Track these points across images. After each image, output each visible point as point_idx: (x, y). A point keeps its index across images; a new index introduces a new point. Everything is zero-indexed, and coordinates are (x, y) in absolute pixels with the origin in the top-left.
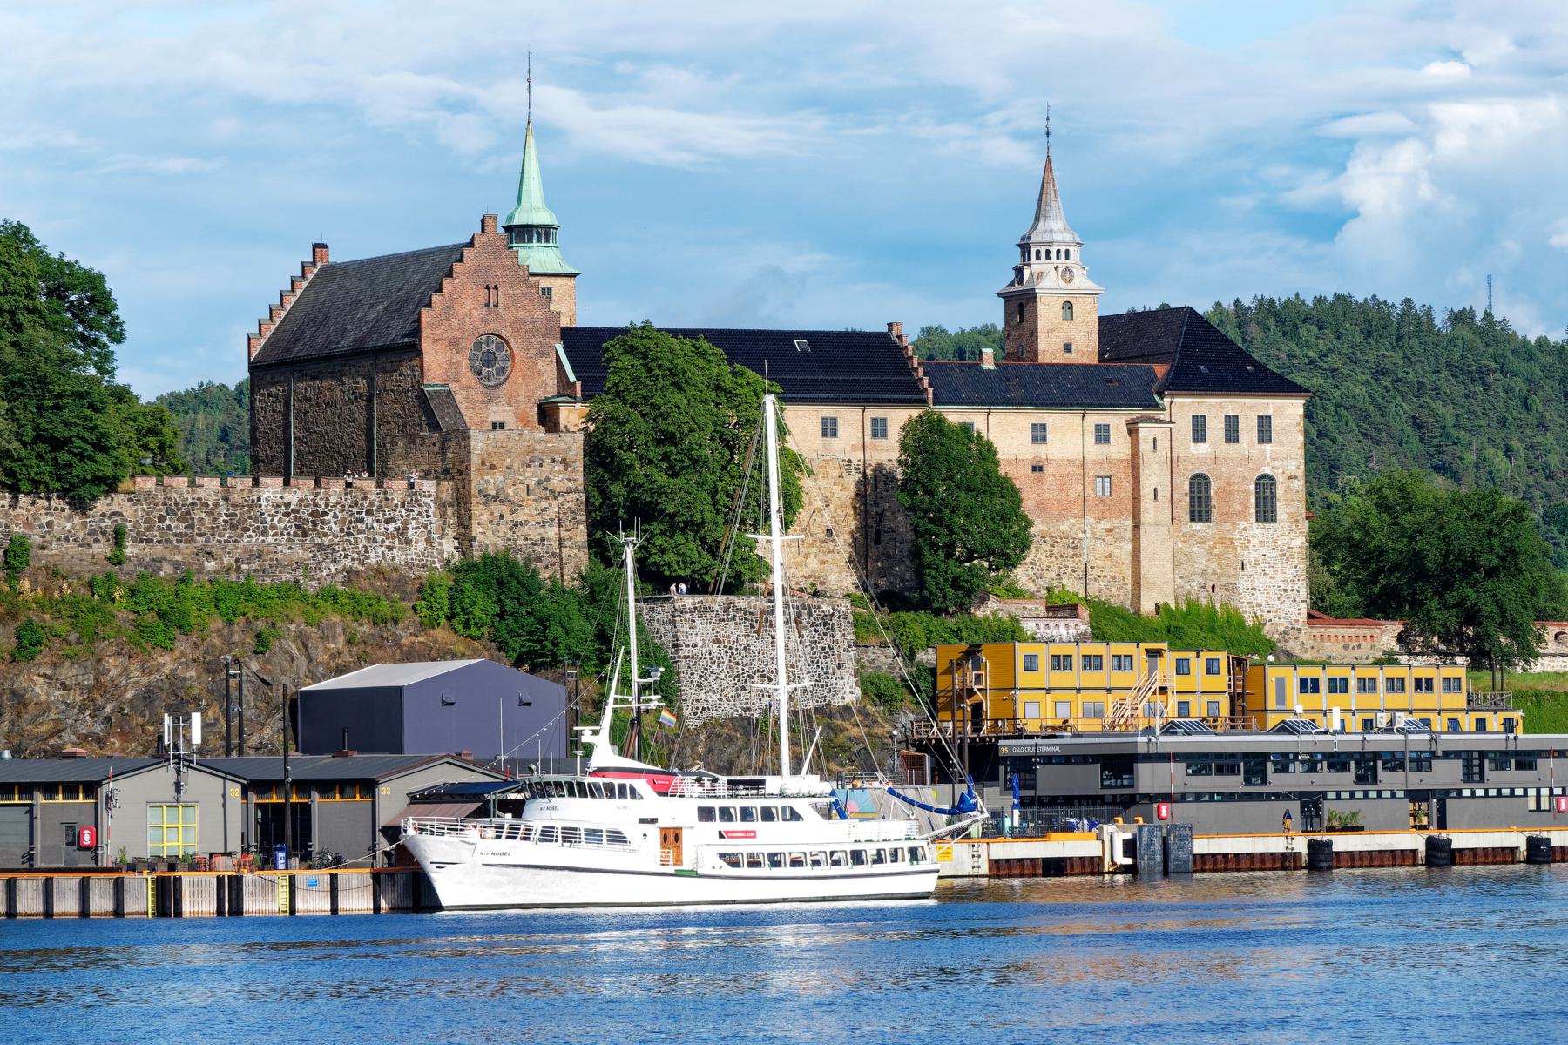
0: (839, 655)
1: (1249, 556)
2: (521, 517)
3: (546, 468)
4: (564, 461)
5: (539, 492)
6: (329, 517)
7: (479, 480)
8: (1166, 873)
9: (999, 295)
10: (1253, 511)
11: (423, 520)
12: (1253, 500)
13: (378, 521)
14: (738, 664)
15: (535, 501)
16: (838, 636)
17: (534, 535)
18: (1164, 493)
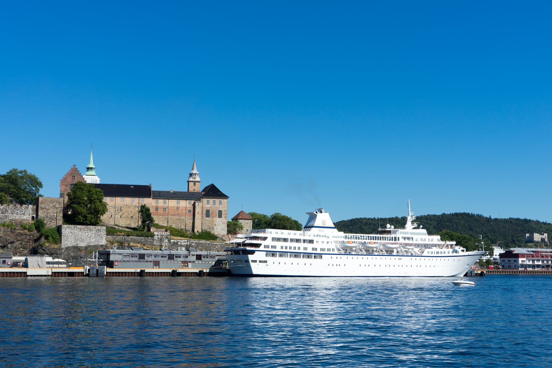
0: (102, 236)
1: (216, 223)
2: (49, 211)
3: (55, 203)
4: (59, 203)
5: (53, 208)
6: (9, 211)
7: (40, 205)
8: (97, 276)
10: (218, 216)
11: (29, 212)
12: (218, 214)
14: (76, 237)
16: (102, 233)
17: (52, 215)
18: (200, 213)
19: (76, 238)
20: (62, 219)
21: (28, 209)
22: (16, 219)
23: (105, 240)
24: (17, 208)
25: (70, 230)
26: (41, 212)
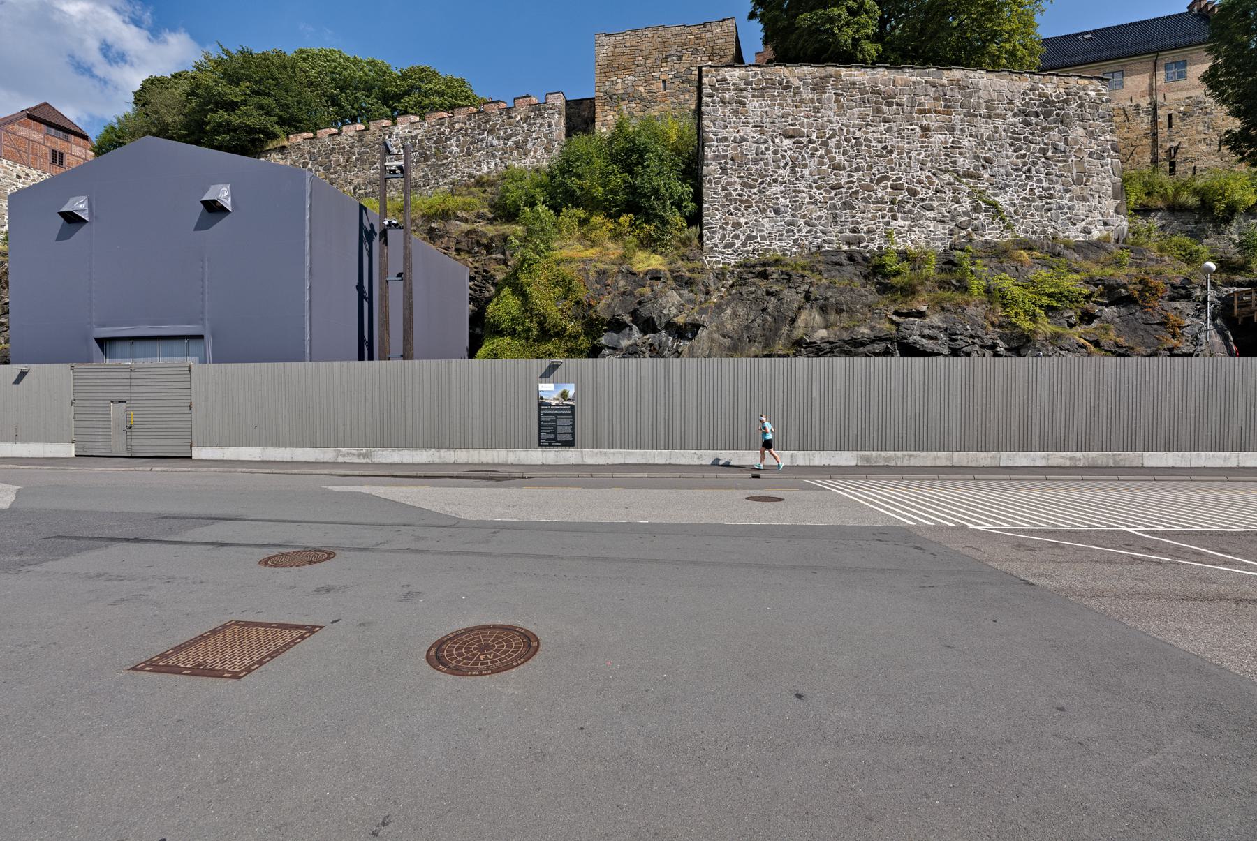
0: (1081, 161)
13: (498, 138)
14: (837, 167)
15: (674, 95)
16: (1077, 132)
19: (843, 177)
21: (541, 116)
22: (481, 177)
23: (1110, 204)
24: (487, 122)
25: (777, 111)
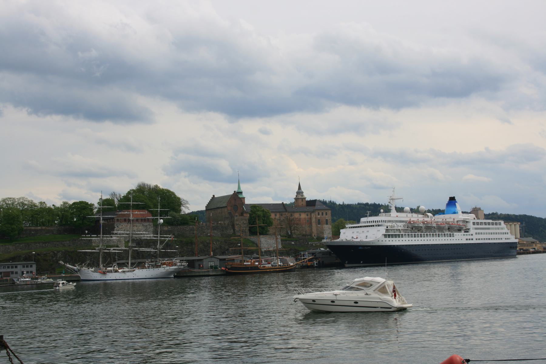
1: (325, 229)
4: (246, 220)
9: (294, 199)
18: (315, 222)
20: (248, 231)
26: (237, 227)
